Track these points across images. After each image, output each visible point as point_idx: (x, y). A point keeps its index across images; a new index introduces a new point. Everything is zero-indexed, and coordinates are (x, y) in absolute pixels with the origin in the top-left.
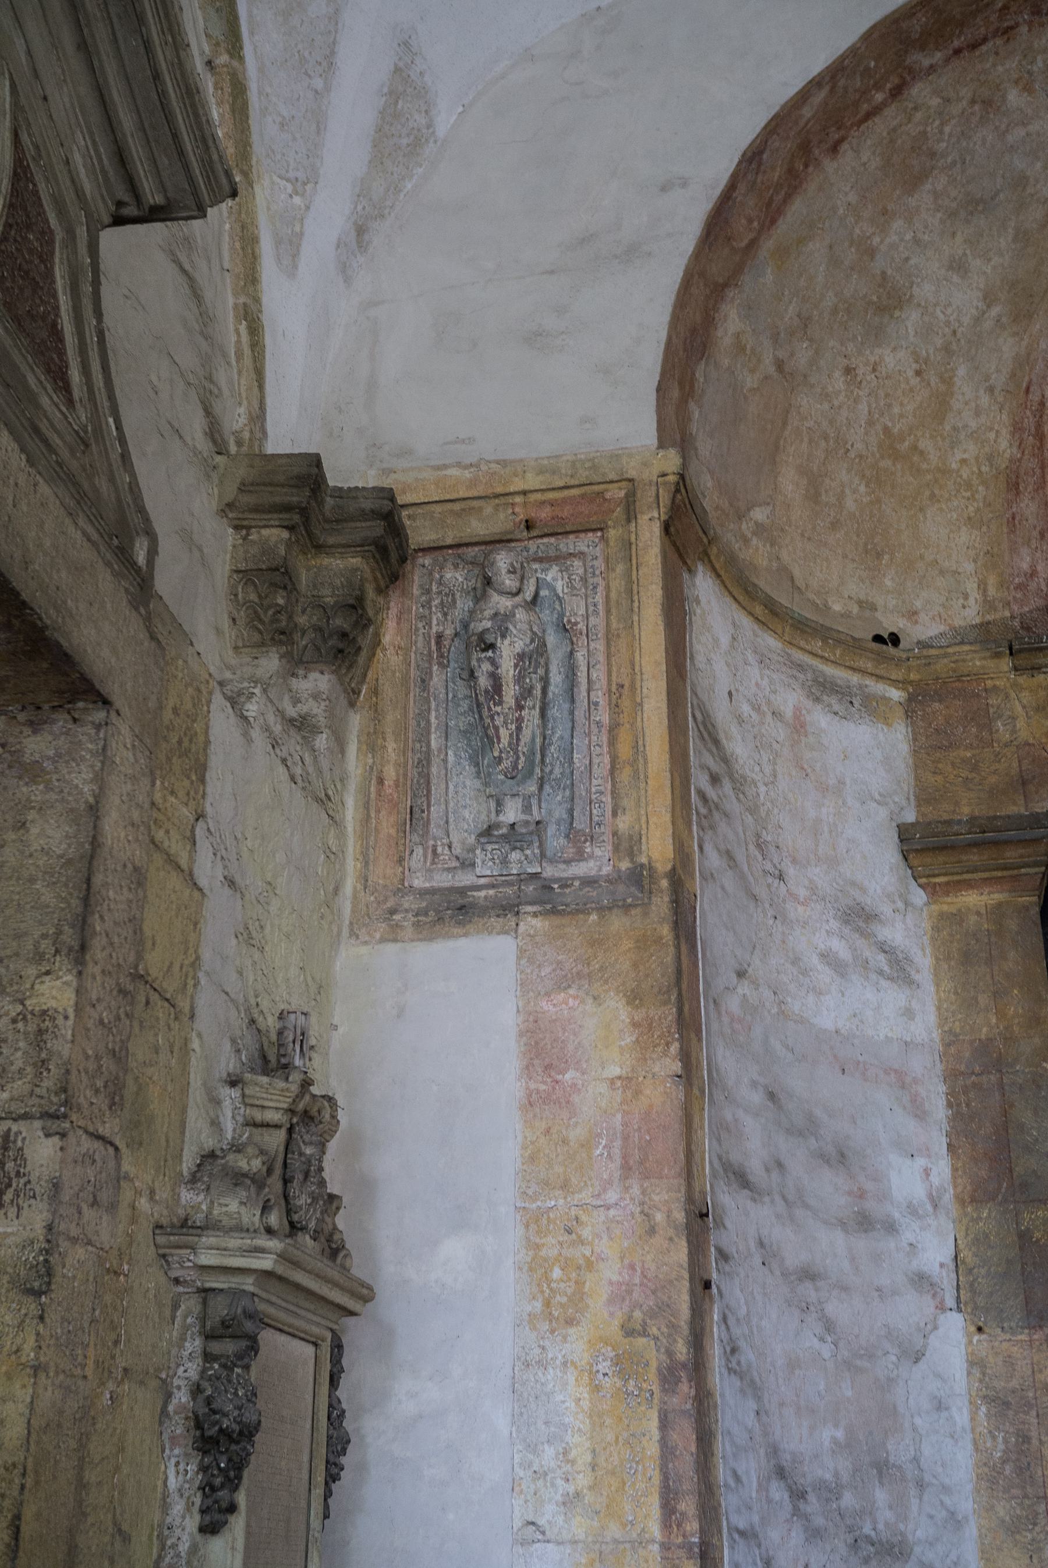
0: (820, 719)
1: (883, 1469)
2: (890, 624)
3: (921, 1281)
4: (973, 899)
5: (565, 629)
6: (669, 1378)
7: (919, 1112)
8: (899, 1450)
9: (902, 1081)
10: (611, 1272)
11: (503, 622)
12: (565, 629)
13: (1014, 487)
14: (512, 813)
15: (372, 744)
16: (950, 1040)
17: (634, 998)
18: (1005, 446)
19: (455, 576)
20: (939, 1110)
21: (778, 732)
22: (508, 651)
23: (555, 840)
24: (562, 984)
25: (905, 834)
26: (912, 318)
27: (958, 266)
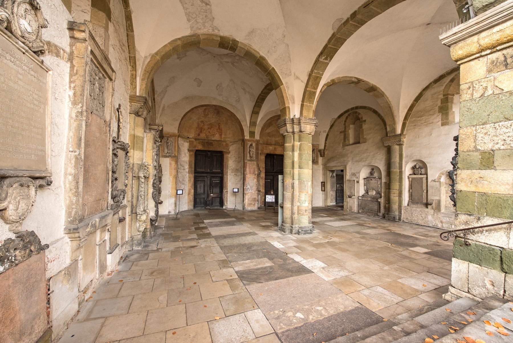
0: (184, 143)
1: (184, 180)
2: (189, 136)
3: (186, 172)
4: (191, 153)
5: (172, 142)
6: (176, 178)
7: (187, 164)
8: (184, 180)
9: (187, 163)
10: (173, 174)
11: (169, 142)
12: (172, 142)
13: (197, 128)
14: (169, 152)
15: (161, 147)
16: (189, 160)
17: (175, 162)
18: (197, 126)
19: (166, 138)
20: (188, 164)
21: (182, 144)
22: (169, 143)
23: (171, 153)
24: (172, 161)
25: (188, 149)
26: (192, 119)
27: (195, 117)
